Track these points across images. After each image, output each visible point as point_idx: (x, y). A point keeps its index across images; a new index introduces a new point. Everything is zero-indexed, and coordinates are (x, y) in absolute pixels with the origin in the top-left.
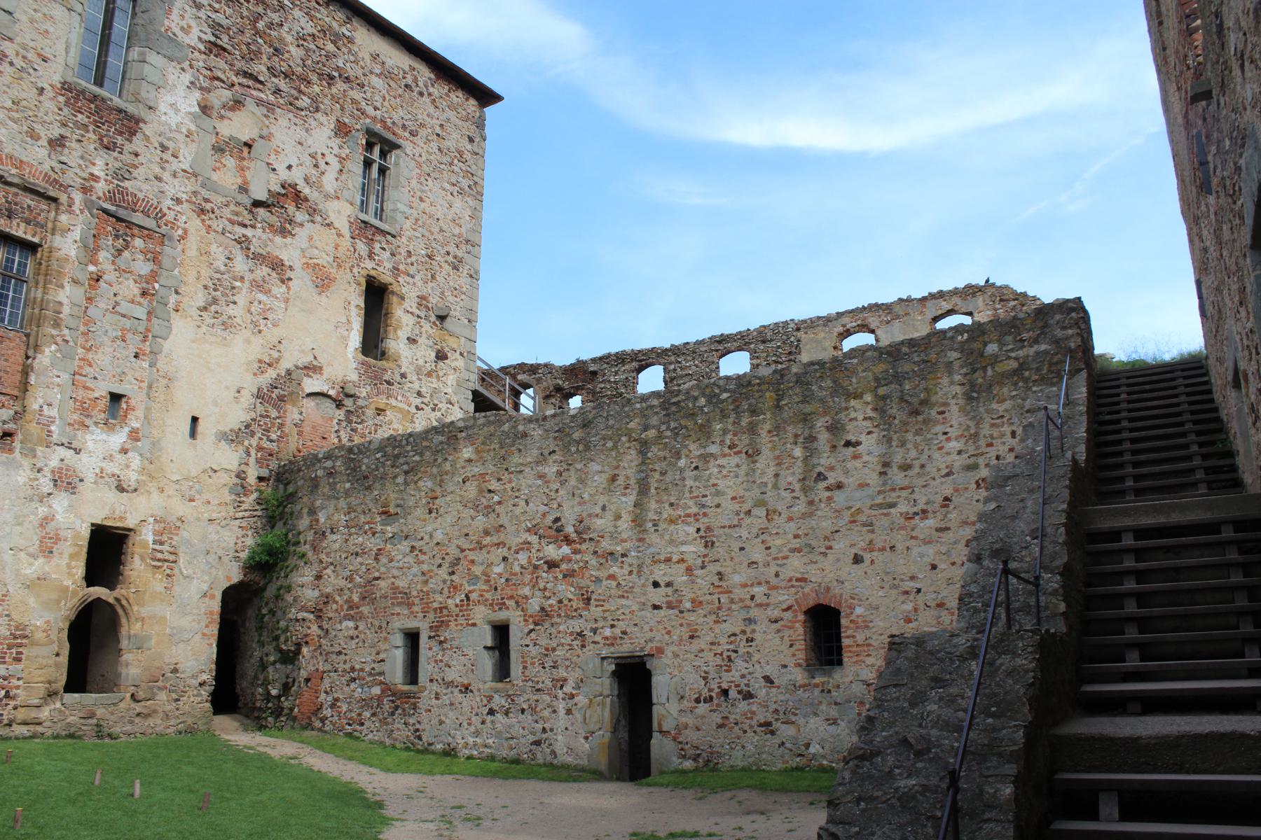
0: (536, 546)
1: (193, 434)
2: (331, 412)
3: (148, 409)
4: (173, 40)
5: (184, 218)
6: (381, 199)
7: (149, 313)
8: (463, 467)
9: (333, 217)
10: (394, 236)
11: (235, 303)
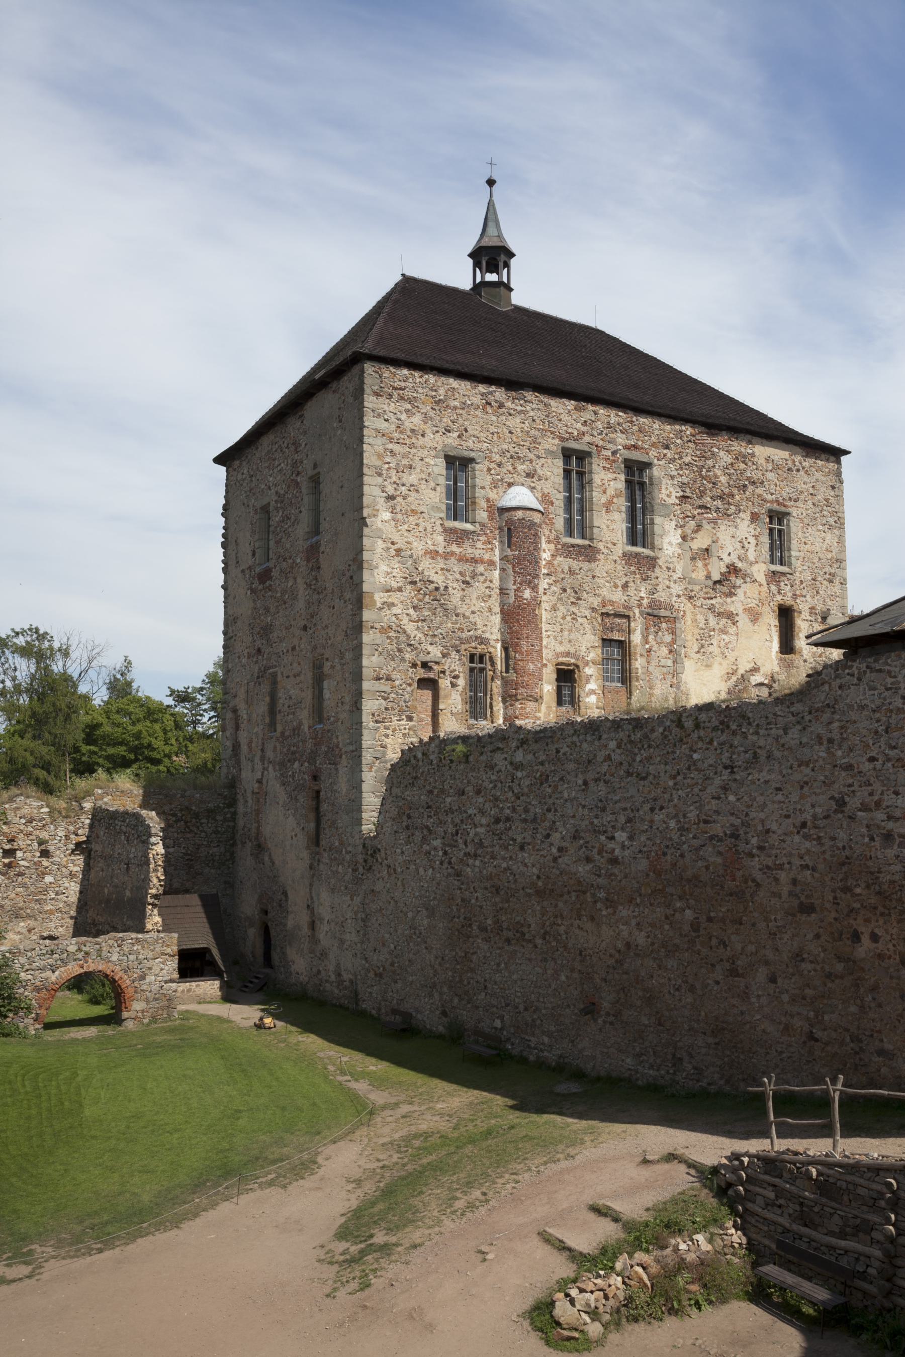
10: (791, 574)
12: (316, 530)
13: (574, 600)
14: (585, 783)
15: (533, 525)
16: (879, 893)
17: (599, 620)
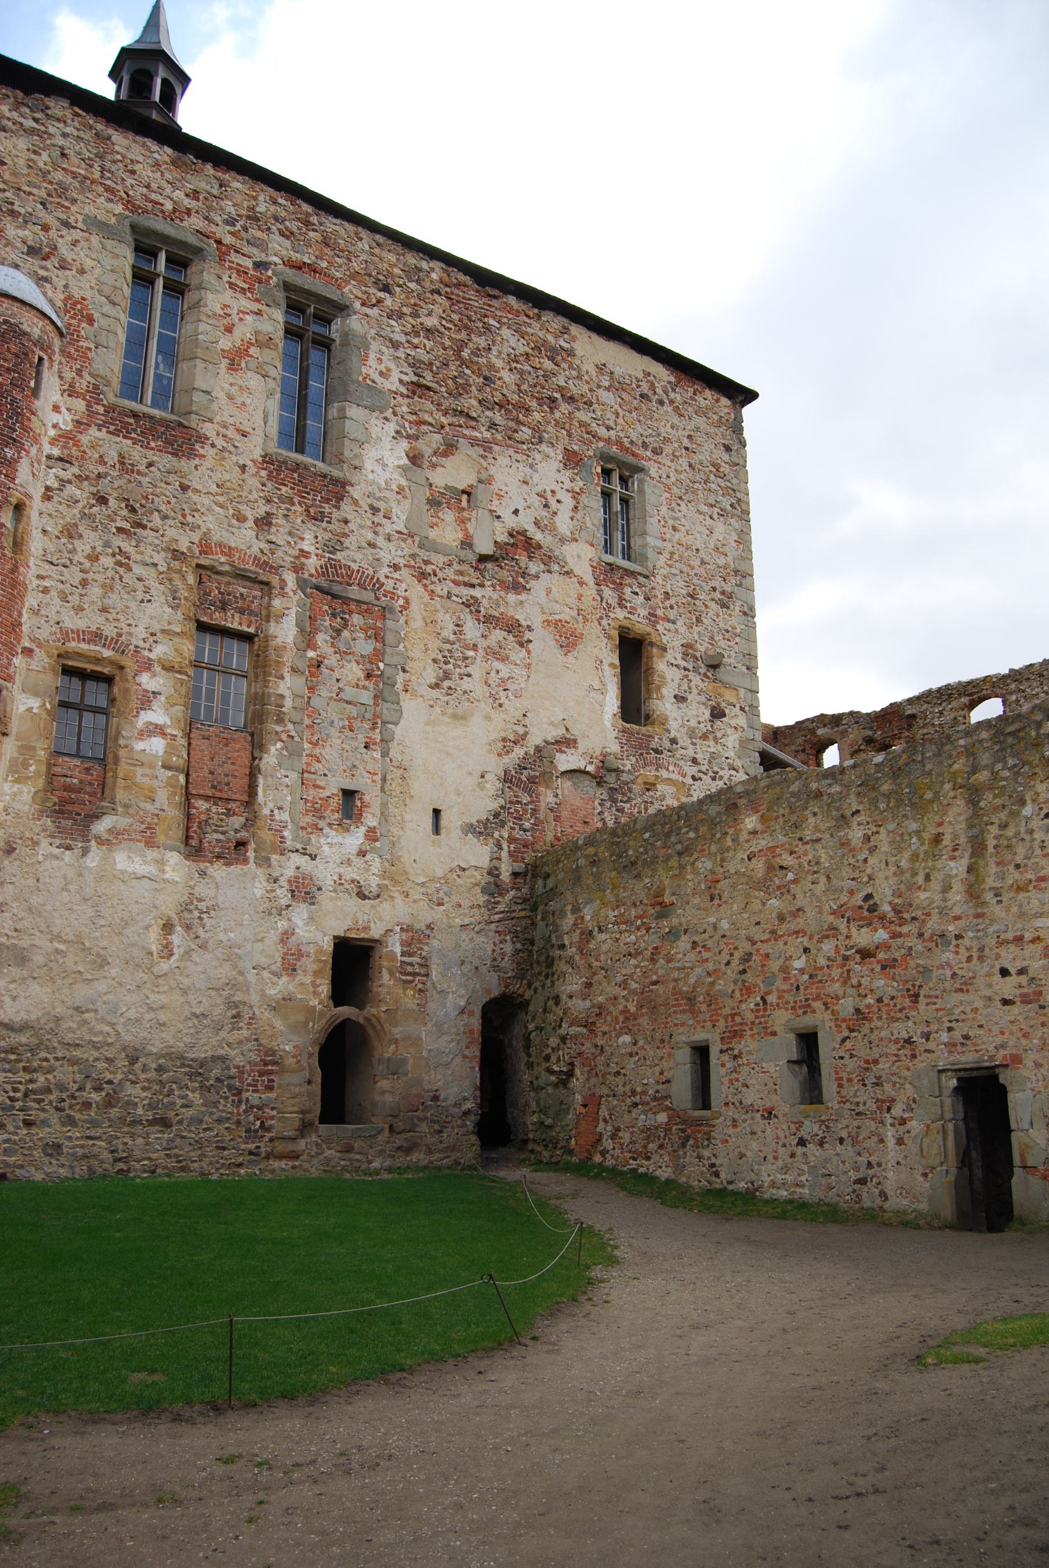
0: (845, 931)
1: (437, 829)
2: (591, 791)
3: (384, 805)
4: (373, 389)
5: (404, 586)
6: (627, 536)
7: (376, 697)
8: (748, 841)
9: (571, 563)
10: (646, 577)
11: (469, 675)
13: (126, 525)
17: (191, 579)
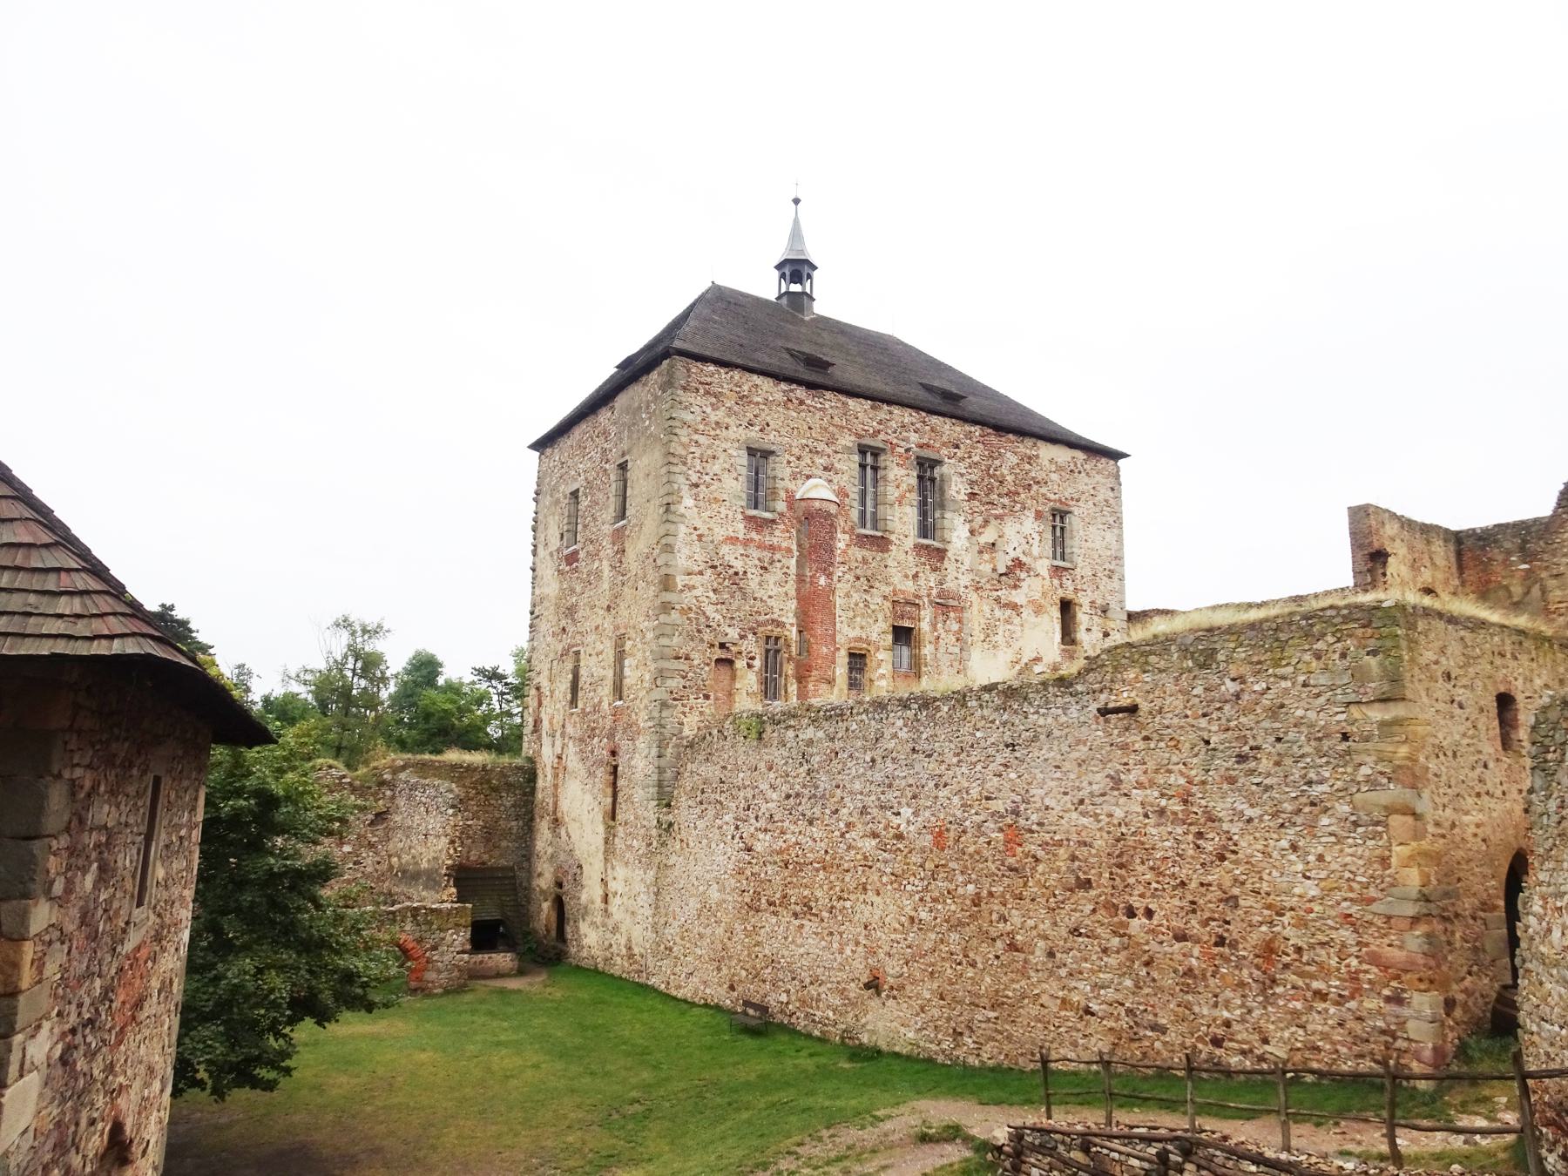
12: (622, 514)
14: (873, 761)
15: (829, 515)
16: (1152, 868)
